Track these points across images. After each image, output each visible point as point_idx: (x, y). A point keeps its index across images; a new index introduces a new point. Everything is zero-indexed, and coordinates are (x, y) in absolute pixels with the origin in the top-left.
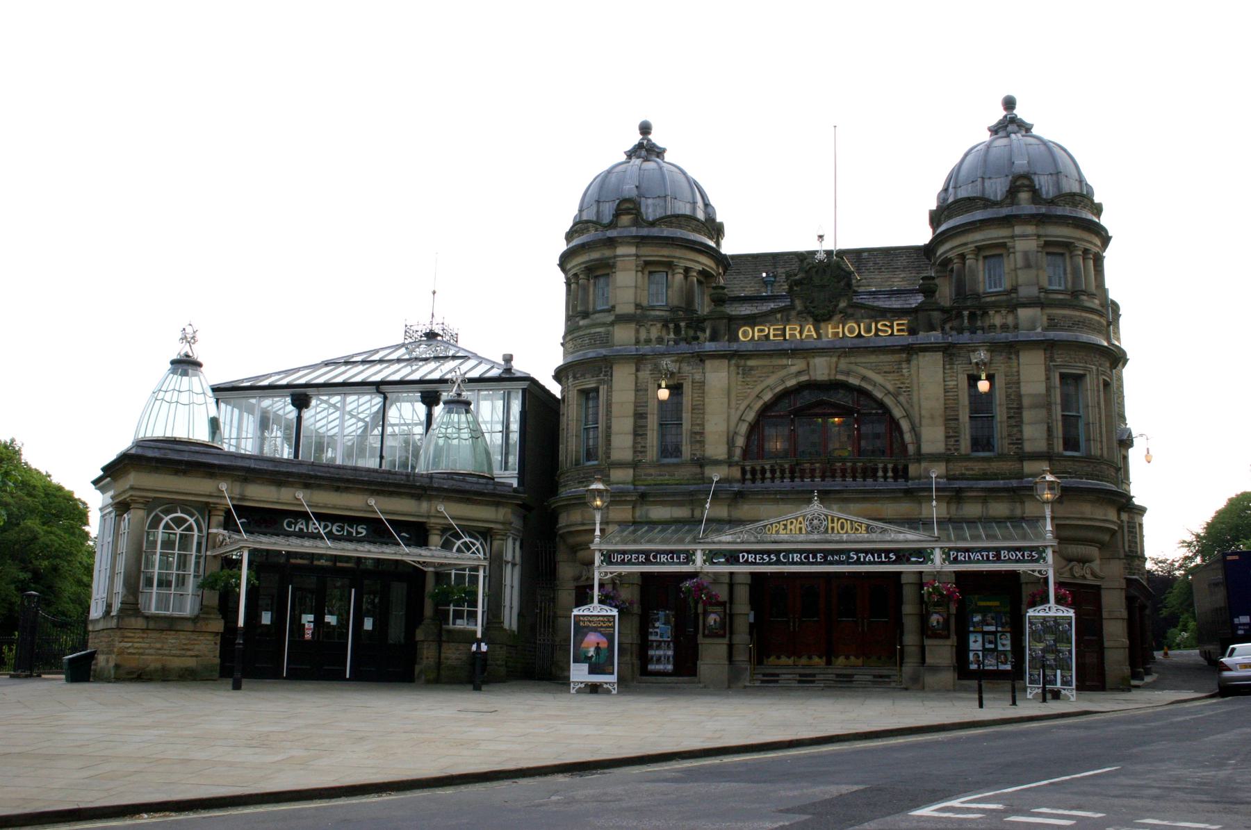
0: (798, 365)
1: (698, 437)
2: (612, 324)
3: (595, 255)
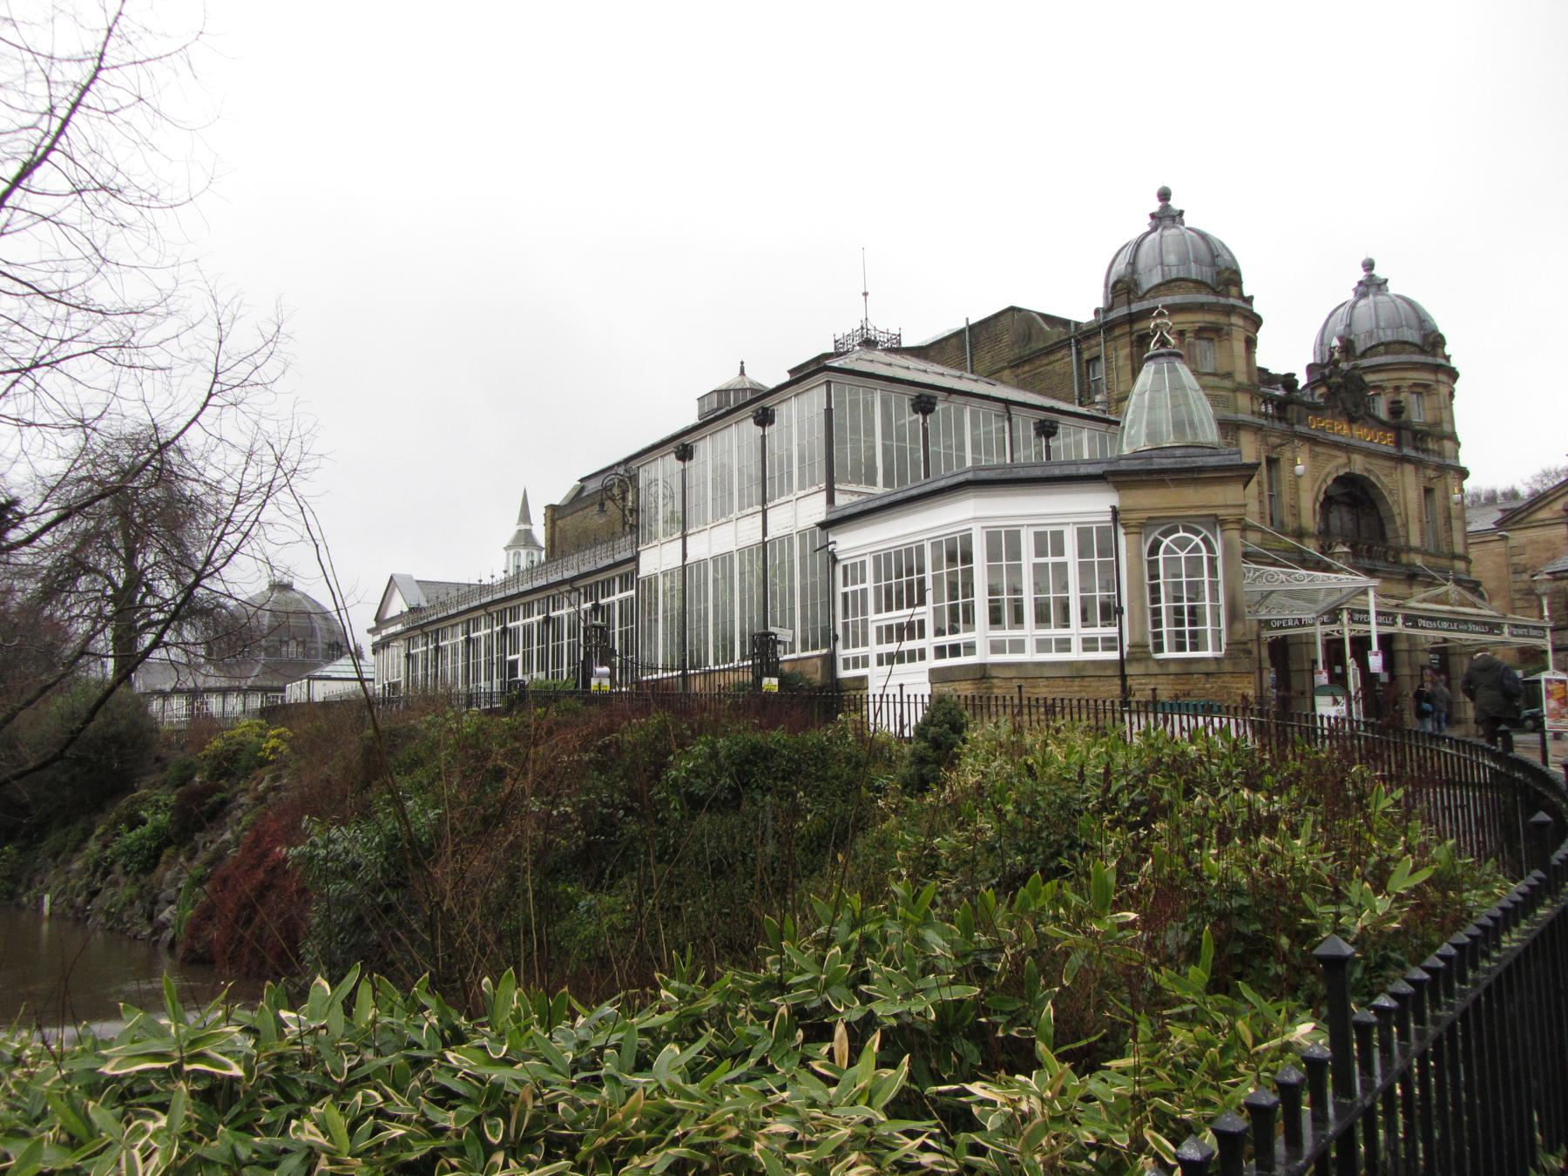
0: (1342, 458)
1: (1296, 512)
2: (1235, 391)
3: (1210, 318)
